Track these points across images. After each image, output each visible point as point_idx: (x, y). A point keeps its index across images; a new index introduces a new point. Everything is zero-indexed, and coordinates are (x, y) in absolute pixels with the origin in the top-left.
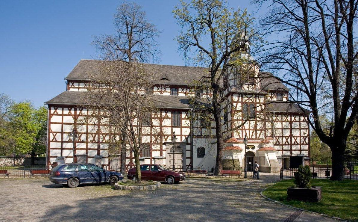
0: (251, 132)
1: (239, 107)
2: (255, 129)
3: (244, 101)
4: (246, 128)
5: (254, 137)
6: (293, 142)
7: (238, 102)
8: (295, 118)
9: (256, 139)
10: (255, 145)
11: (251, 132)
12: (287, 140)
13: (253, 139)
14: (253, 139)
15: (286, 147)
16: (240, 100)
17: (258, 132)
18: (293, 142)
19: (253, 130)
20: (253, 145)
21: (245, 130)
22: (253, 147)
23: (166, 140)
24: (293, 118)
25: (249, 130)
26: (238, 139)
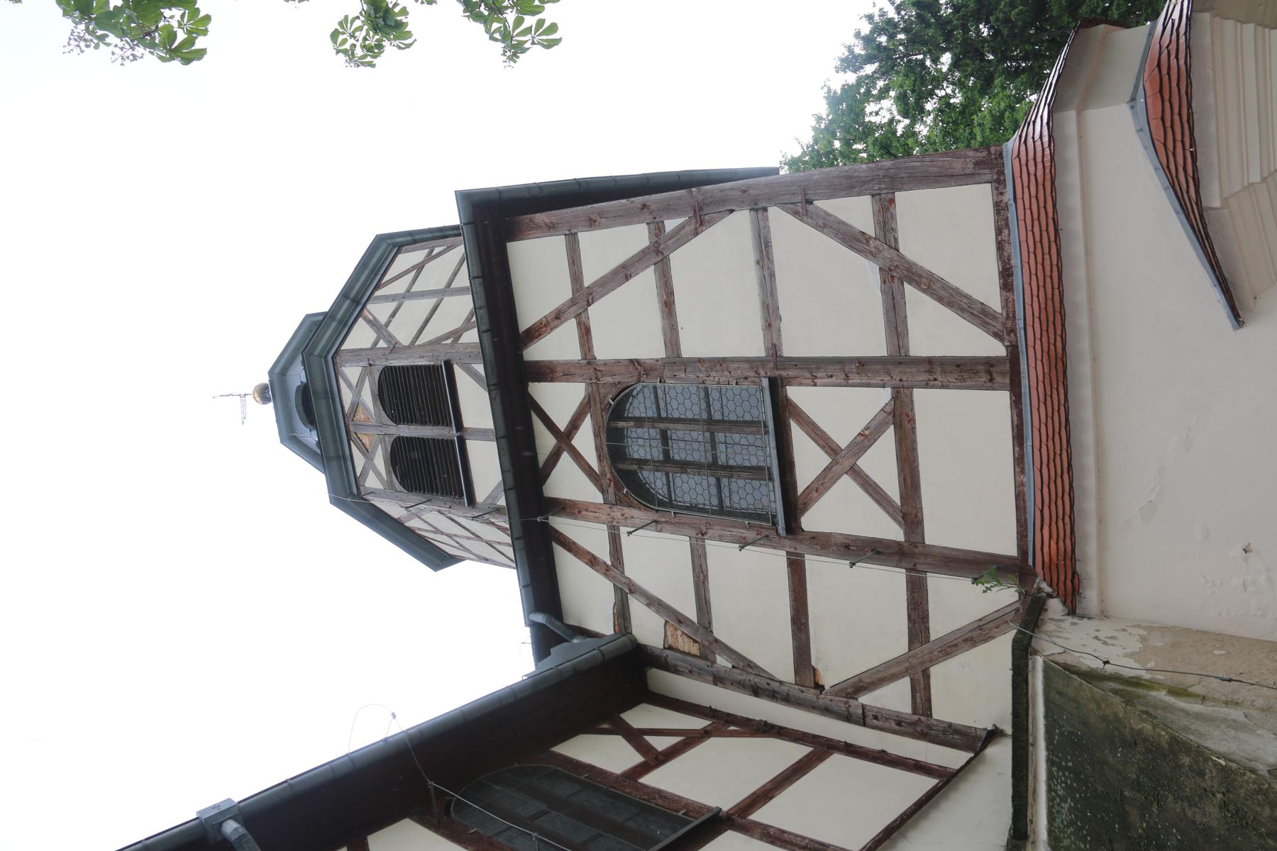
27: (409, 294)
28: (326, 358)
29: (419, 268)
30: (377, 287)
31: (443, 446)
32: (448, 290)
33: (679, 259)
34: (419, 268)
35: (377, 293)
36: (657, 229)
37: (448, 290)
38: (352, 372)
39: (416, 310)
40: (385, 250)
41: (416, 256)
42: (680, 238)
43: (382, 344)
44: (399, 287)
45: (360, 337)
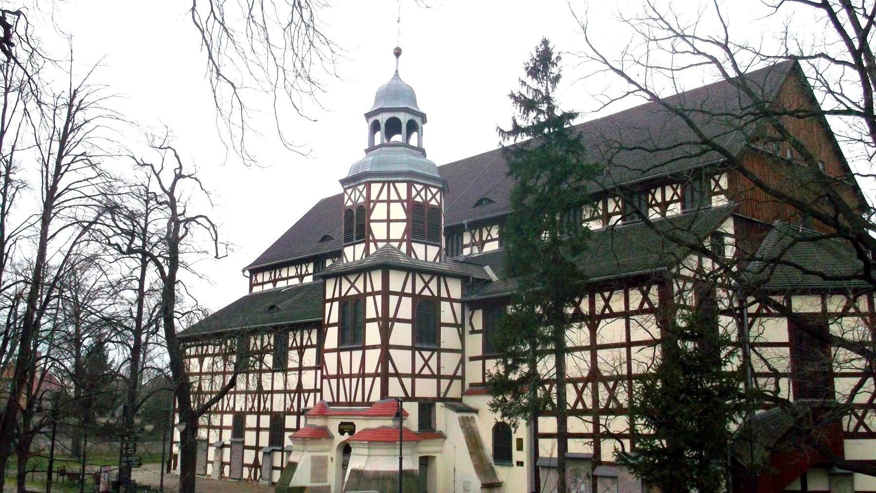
0: (354, 380)
1: (333, 313)
2: (362, 375)
3: (343, 295)
5: (359, 399)
6: (602, 404)
7: (332, 300)
8: (607, 301)
10: (356, 422)
11: (354, 380)
12: (580, 393)
13: (358, 404)
14: (358, 404)
15: (575, 424)
16: (337, 295)
17: (368, 381)
18: (602, 404)
19: (358, 376)
20: (352, 424)
21: (344, 376)
23: (306, 402)
24: (600, 304)
25: (351, 376)
26: (329, 403)
31: (351, 239)
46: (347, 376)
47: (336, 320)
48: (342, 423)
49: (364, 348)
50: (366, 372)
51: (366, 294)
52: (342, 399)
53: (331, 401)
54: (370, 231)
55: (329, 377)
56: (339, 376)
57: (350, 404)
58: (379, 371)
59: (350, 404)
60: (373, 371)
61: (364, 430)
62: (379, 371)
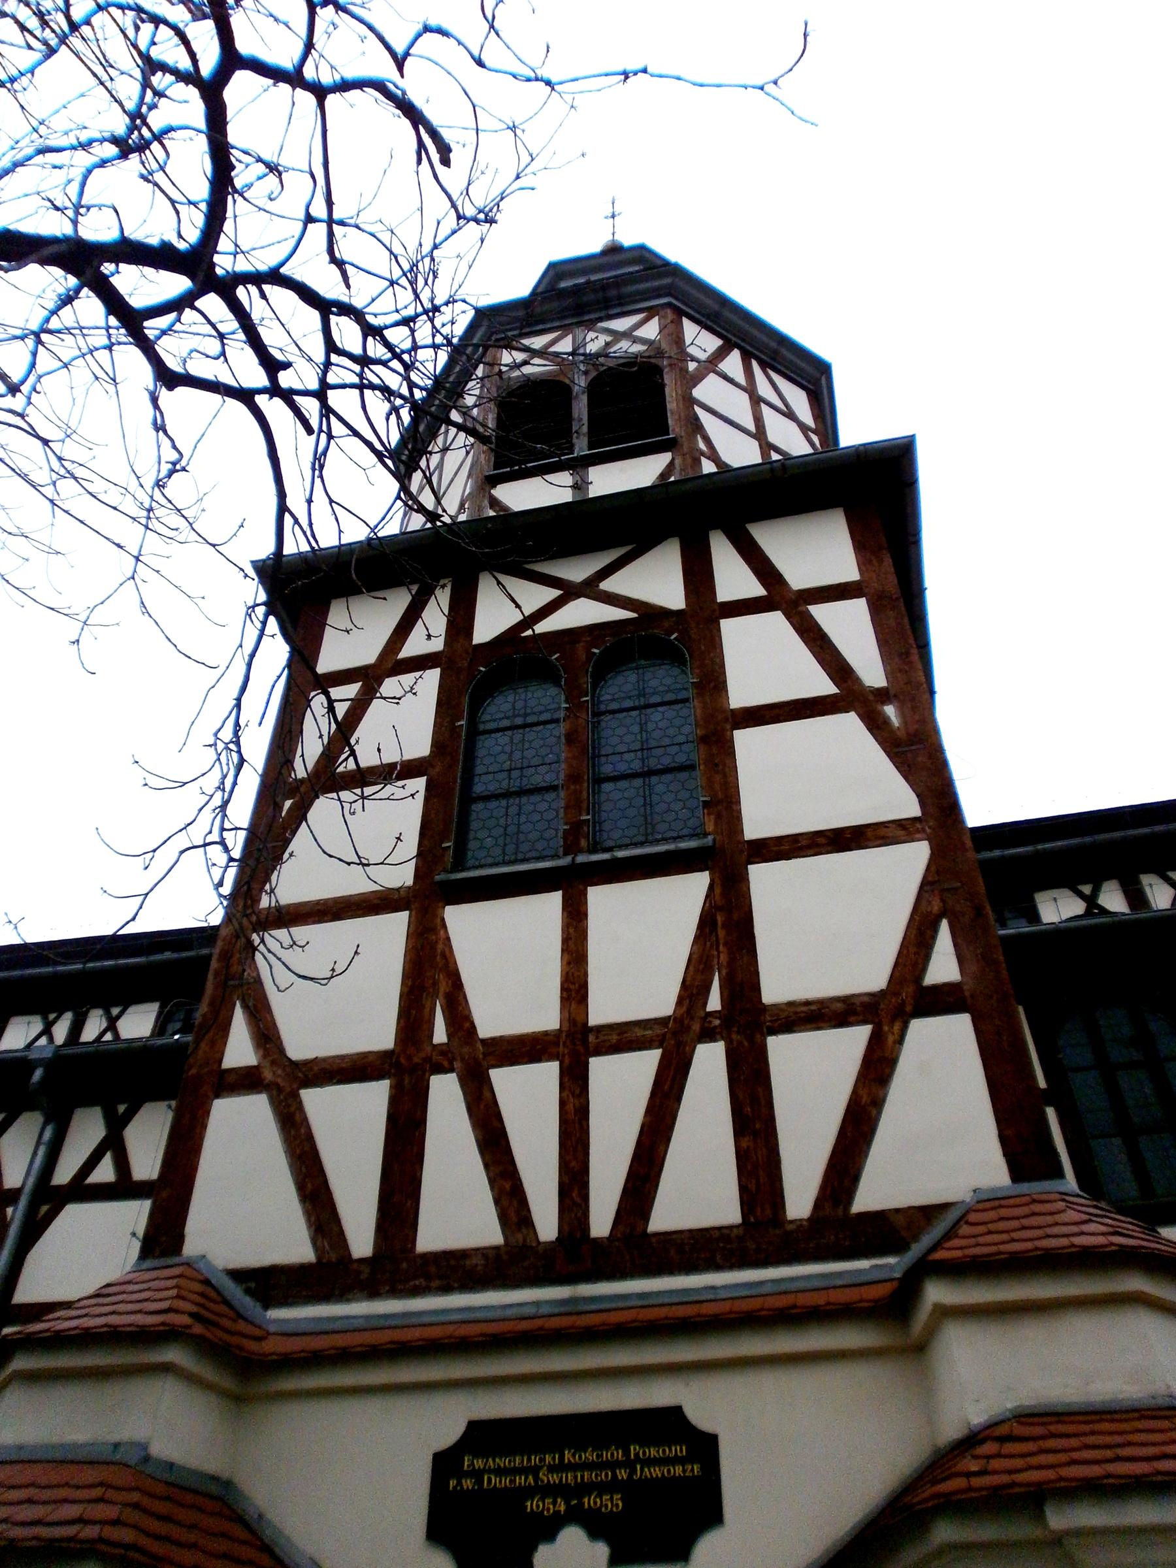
4: (492, 1018)
5: (700, 1188)
9: (761, 1230)
10: (705, 1404)
19: (673, 1039)
20: (669, 1423)
21: (477, 1058)
22: (661, 1464)
25: (574, 1045)
27: (756, 401)
28: (669, 294)
29: (790, 415)
30: (764, 366)
32: (766, 447)
33: (848, 726)
34: (790, 415)
35: (755, 364)
36: (882, 695)
37: (766, 447)
38: (651, 330)
39: (738, 406)
40: (814, 376)
41: (804, 412)
42: (875, 724)
43: (692, 366)
44: (764, 388)
45: (700, 342)
46: (523, 1049)
47: (419, 745)
48: (482, 1436)
49: (729, 860)
50: (776, 987)
51: (705, 611)
52: (456, 1211)
53: (293, 1245)
54: (697, 427)
55: (286, 1081)
56: (432, 1044)
57: (576, 1255)
58: (944, 966)
59: (576, 1255)
60: (871, 973)
61: (1025, 1416)
62: (944, 966)
